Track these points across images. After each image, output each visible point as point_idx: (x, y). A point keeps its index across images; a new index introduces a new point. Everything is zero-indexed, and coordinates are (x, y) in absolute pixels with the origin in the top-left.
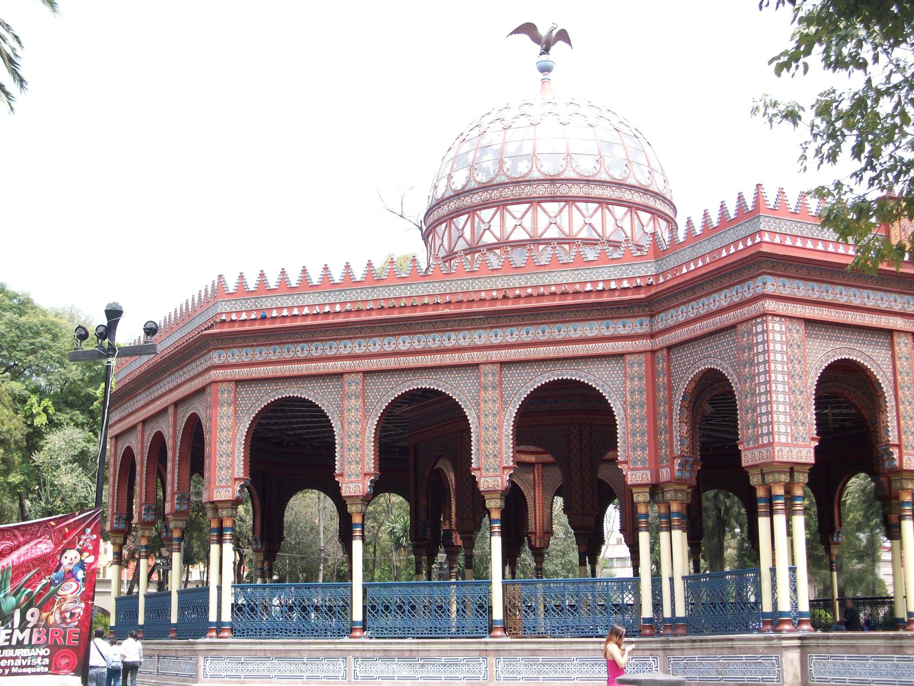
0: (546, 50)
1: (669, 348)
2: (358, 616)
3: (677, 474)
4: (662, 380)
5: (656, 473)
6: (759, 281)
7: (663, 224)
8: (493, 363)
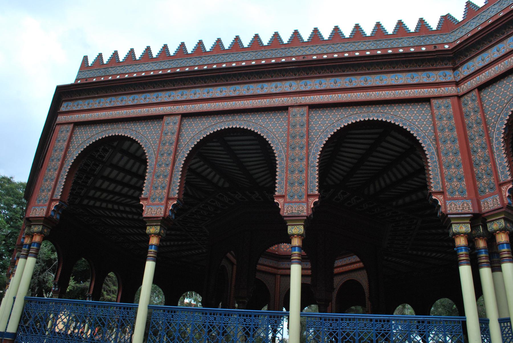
3: (506, 201)
4: (472, 118)
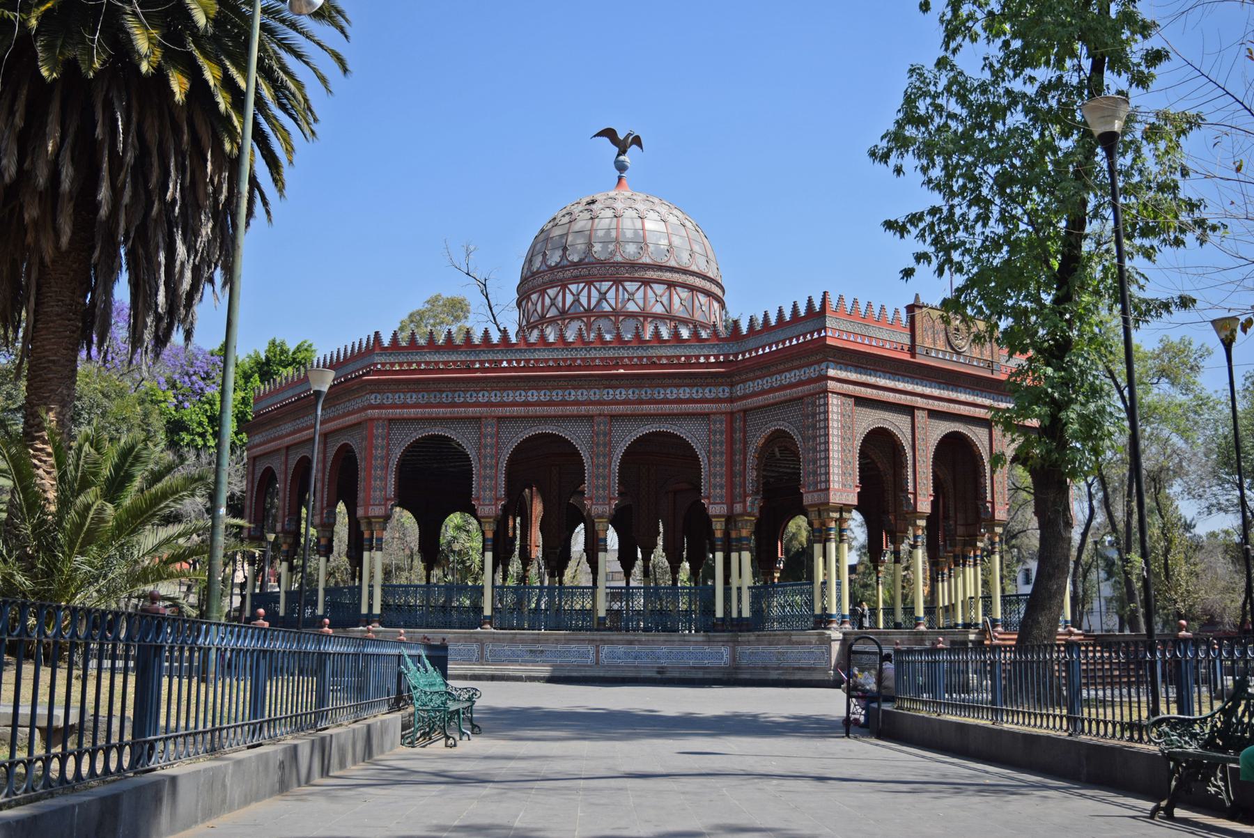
0: (623, 152)
1: (745, 411)
2: (487, 611)
4: (738, 435)
5: (731, 508)
6: (823, 366)
7: (716, 305)
8: (605, 416)
